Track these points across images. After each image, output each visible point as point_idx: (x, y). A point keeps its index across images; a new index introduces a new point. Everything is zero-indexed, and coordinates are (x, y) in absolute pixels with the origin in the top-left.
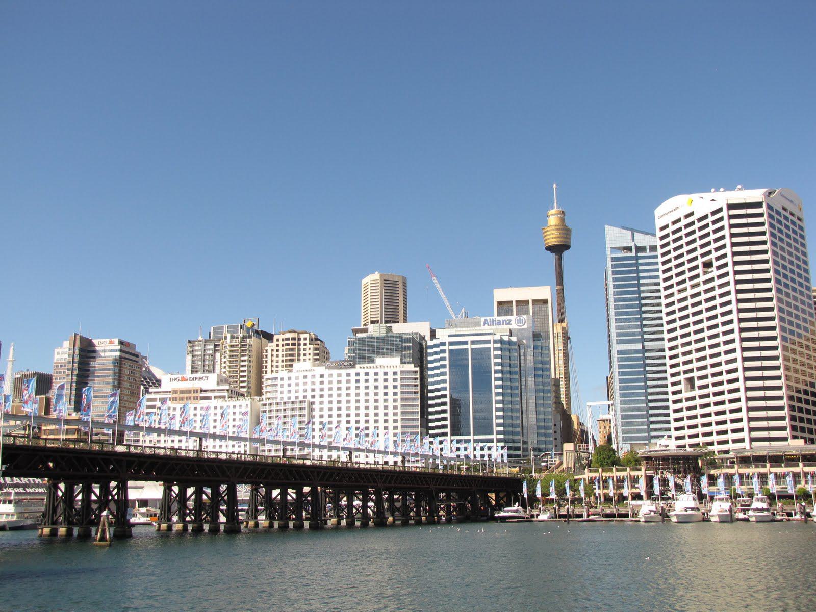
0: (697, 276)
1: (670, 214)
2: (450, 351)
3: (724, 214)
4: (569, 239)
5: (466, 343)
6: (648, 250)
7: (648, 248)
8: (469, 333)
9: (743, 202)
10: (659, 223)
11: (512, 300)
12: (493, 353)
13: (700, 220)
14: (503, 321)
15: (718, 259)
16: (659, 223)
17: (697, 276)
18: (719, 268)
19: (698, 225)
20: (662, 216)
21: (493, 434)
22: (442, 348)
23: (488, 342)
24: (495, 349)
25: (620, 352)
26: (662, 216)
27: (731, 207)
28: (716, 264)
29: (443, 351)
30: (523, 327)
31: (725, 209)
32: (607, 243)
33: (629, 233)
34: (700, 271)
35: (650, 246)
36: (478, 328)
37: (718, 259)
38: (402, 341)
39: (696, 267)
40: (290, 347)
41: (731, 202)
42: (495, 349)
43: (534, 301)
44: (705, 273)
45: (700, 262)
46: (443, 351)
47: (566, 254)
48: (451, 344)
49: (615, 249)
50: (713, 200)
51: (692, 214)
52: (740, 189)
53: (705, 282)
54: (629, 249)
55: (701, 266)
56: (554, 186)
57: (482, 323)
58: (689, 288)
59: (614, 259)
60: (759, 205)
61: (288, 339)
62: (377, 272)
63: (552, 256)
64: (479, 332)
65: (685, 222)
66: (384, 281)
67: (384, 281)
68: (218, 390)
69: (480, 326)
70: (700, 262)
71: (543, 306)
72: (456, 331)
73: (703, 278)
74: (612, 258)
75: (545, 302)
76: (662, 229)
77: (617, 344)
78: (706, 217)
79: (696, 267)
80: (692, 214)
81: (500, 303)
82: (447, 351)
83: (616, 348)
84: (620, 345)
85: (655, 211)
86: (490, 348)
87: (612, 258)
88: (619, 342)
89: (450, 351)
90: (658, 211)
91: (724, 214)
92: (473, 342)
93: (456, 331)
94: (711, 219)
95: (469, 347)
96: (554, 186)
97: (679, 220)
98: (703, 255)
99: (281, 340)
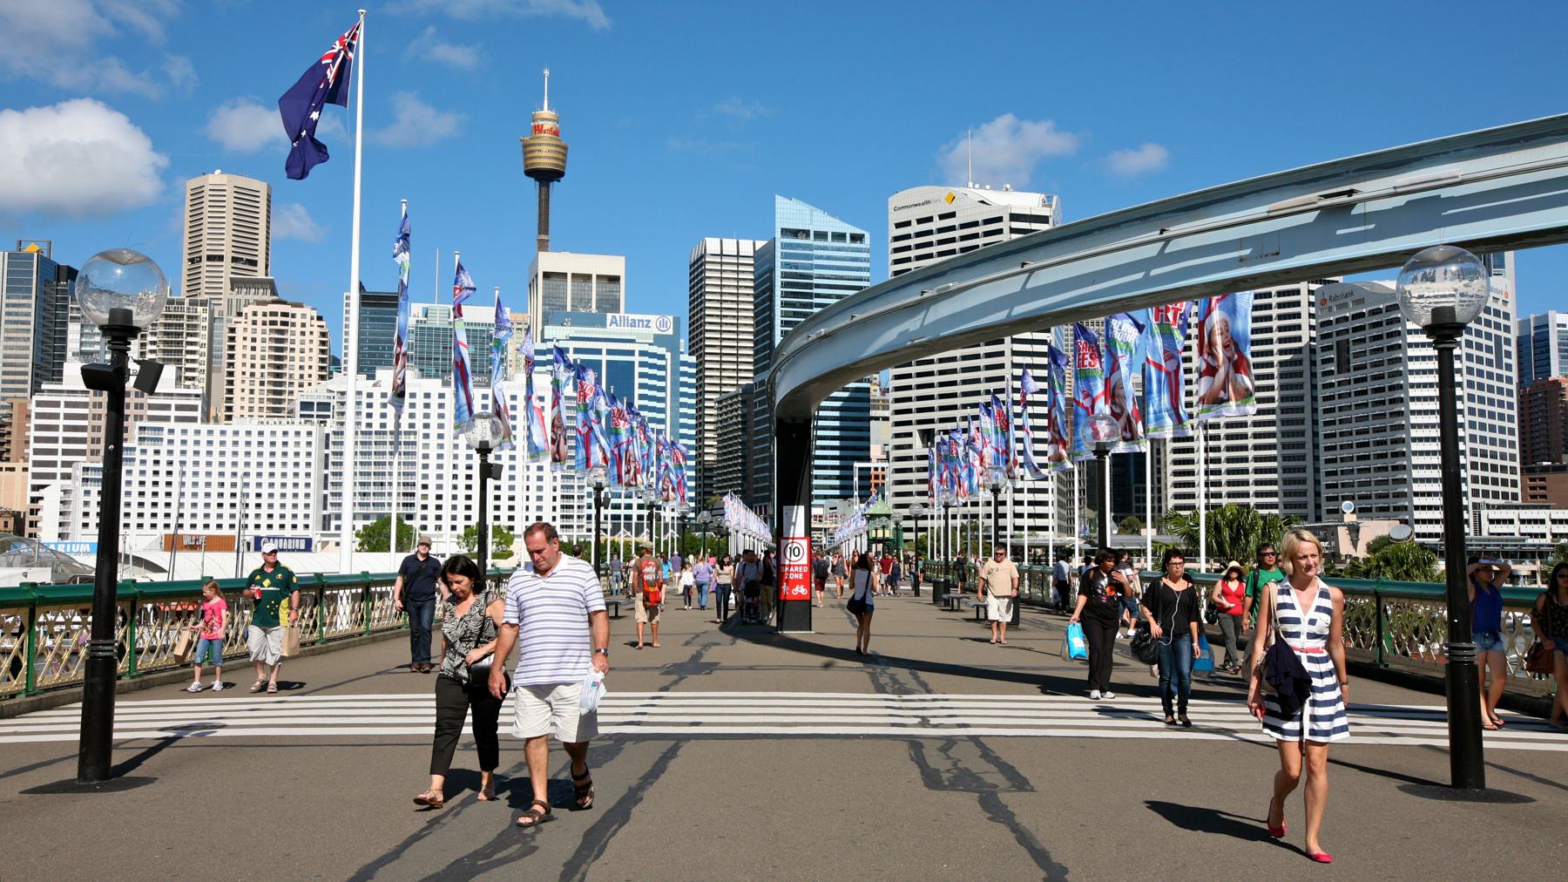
1: (913, 208)
4: (564, 161)
5: (599, 352)
8: (593, 336)
9: (1027, 212)
12: (638, 370)
13: (963, 226)
14: (639, 321)
16: (897, 217)
20: (899, 209)
23: (631, 353)
24: (642, 364)
26: (899, 209)
30: (667, 333)
31: (1006, 218)
32: (777, 220)
36: (601, 329)
40: (279, 327)
42: (642, 364)
43: (599, 277)
47: (555, 186)
50: (982, 202)
51: (952, 215)
54: (806, 233)
56: (546, 73)
57: (608, 322)
59: (784, 246)
61: (274, 314)
63: (532, 184)
64: (605, 336)
65: (937, 224)
68: (179, 395)
69: (604, 325)
71: (611, 286)
72: (576, 332)
75: (614, 279)
76: (898, 225)
78: (975, 224)
80: (952, 215)
81: (547, 275)
86: (633, 363)
90: (895, 201)
91: (1005, 225)
92: (610, 352)
93: (576, 332)
95: (604, 358)
96: (546, 73)
97: (930, 219)
99: (260, 314)
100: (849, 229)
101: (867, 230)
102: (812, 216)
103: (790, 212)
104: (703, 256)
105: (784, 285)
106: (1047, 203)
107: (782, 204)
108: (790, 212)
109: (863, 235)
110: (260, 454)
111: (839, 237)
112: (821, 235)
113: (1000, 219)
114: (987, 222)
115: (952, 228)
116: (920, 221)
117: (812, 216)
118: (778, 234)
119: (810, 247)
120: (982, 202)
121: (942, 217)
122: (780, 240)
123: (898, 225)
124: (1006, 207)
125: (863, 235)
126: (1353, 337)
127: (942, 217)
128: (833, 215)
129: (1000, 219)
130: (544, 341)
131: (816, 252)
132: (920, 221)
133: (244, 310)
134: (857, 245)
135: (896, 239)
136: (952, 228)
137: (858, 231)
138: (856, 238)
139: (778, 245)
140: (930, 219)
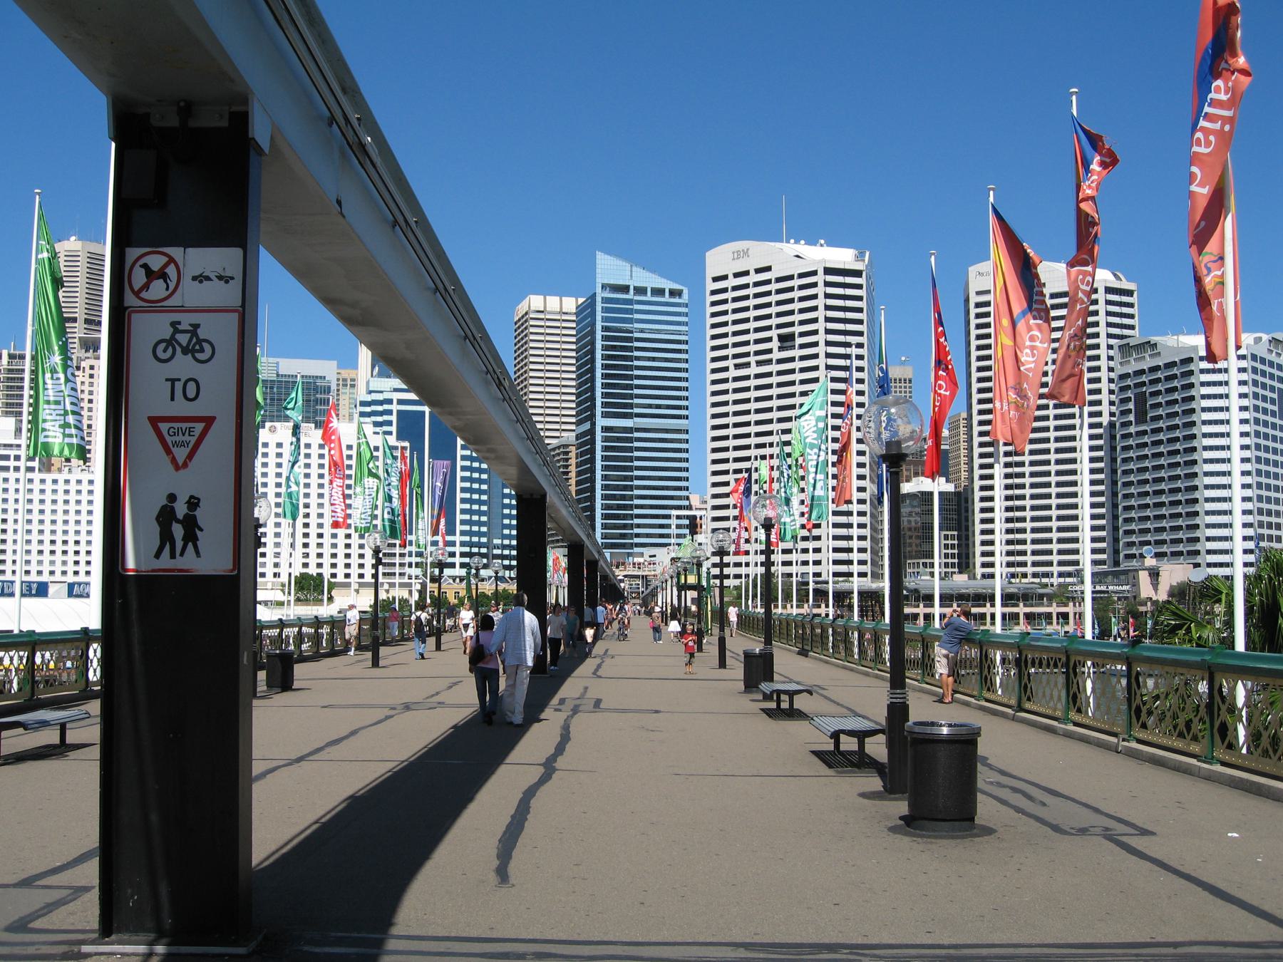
0: (770, 351)
2: (399, 412)
3: (820, 278)
7: (649, 290)
10: (711, 272)
13: (779, 280)
15: (802, 334)
16: (711, 272)
17: (770, 351)
18: (802, 346)
19: (773, 287)
21: (455, 535)
22: (386, 407)
25: (606, 429)
27: (828, 271)
28: (799, 341)
29: (390, 412)
31: (821, 272)
33: (628, 266)
34: (775, 344)
37: (802, 334)
38: (316, 389)
39: (769, 340)
41: (828, 265)
44: (781, 349)
45: (774, 333)
46: (390, 412)
48: (400, 402)
49: (604, 287)
50: (798, 256)
51: (768, 269)
52: (822, 245)
53: (780, 361)
54: (625, 289)
55: (775, 339)
58: (753, 364)
59: (605, 300)
60: (858, 274)
62: (73, 238)
66: (89, 255)
67: (89, 255)
70: (774, 333)
73: (776, 355)
76: (715, 279)
78: (791, 278)
79: (769, 340)
80: (768, 269)
82: (395, 413)
83: (601, 422)
85: (708, 254)
87: (602, 298)
88: (605, 415)
89: (399, 412)
91: (820, 278)
94: (796, 283)
97: (746, 273)
98: (779, 326)
100: (668, 285)
102: (631, 271)
103: (610, 269)
104: (526, 313)
106: (860, 257)
108: (610, 269)
110: (54, 502)
111: (659, 292)
112: (640, 291)
113: (814, 273)
114: (801, 276)
115: (768, 282)
116: (736, 275)
117: (631, 271)
118: (599, 290)
119: (630, 302)
120: (798, 256)
121: (758, 271)
122: (600, 294)
123: (715, 279)
124: (819, 262)
126: (1148, 390)
127: (758, 271)
128: (653, 271)
129: (814, 273)
130: (370, 392)
132: (736, 275)
133: (83, 364)
134: (676, 300)
135: (714, 292)
136: (768, 282)
137: (676, 286)
138: (673, 293)
139: (599, 299)
140: (746, 273)
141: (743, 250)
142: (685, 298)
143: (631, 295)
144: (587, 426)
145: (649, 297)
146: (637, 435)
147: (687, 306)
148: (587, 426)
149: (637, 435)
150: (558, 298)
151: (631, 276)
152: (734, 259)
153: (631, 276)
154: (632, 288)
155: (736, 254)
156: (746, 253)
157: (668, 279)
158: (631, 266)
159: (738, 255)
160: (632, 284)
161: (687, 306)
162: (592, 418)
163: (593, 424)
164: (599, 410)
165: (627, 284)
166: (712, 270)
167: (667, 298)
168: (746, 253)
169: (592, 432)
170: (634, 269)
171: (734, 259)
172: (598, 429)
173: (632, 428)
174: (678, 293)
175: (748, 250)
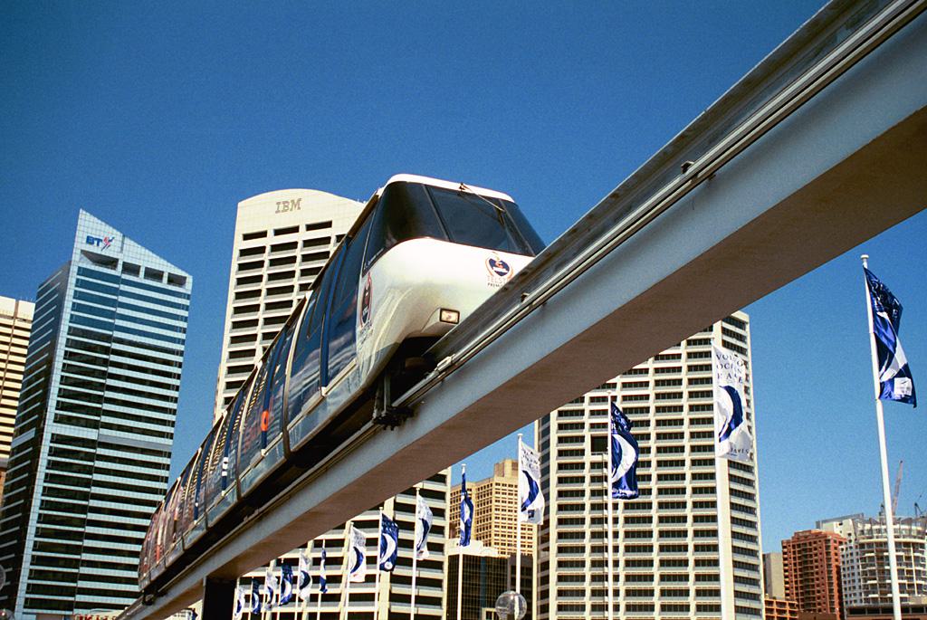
6: (142, 273)
10: (242, 227)
11: (296, 225)
25: (57, 438)
35: (146, 268)
51: (328, 225)
54: (112, 263)
59: (82, 271)
74: (79, 268)
76: (247, 237)
77: (55, 422)
80: (328, 225)
83: (51, 428)
84: (59, 425)
85: (240, 204)
87: (79, 268)
88: (59, 419)
100: (168, 268)
101: (190, 274)
102: (123, 243)
105: (72, 331)
107: (88, 224)
109: (185, 278)
111: (154, 274)
112: (131, 269)
117: (123, 243)
119: (116, 279)
123: (247, 237)
125: (185, 278)
131: (124, 288)
132: (278, 232)
138: (173, 279)
139: (74, 269)
141: (293, 201)
142: (188, 288)
143: (118, 272)
144: (31, 434)
145: (141, 279)
146: (101, 451)
147: (188, 297)
148: (31, 434)
149: (101, 451)
150: (14, 300)
151: (122, 249)
152: (277, 212)
153: (122, 249)
154: (120, 263)
155: (281, 206)
156: (297, 204)
157: (168, 261)
158: (124, 236)
159: (285, 206)
160: (122, 259)
161: (188, 297)
162: (39, 426)
163: (40, 432)
164: (52, 410)
165: (115, 257)
166: (245, 223)
167: (164, 284)
168: (297, 204)
169: (36, 442)
170: (127, 241)
171: (277, 212)
172: (47, 437)
173: (93, 441)
174: (177, 281)
175: (300, 200)
